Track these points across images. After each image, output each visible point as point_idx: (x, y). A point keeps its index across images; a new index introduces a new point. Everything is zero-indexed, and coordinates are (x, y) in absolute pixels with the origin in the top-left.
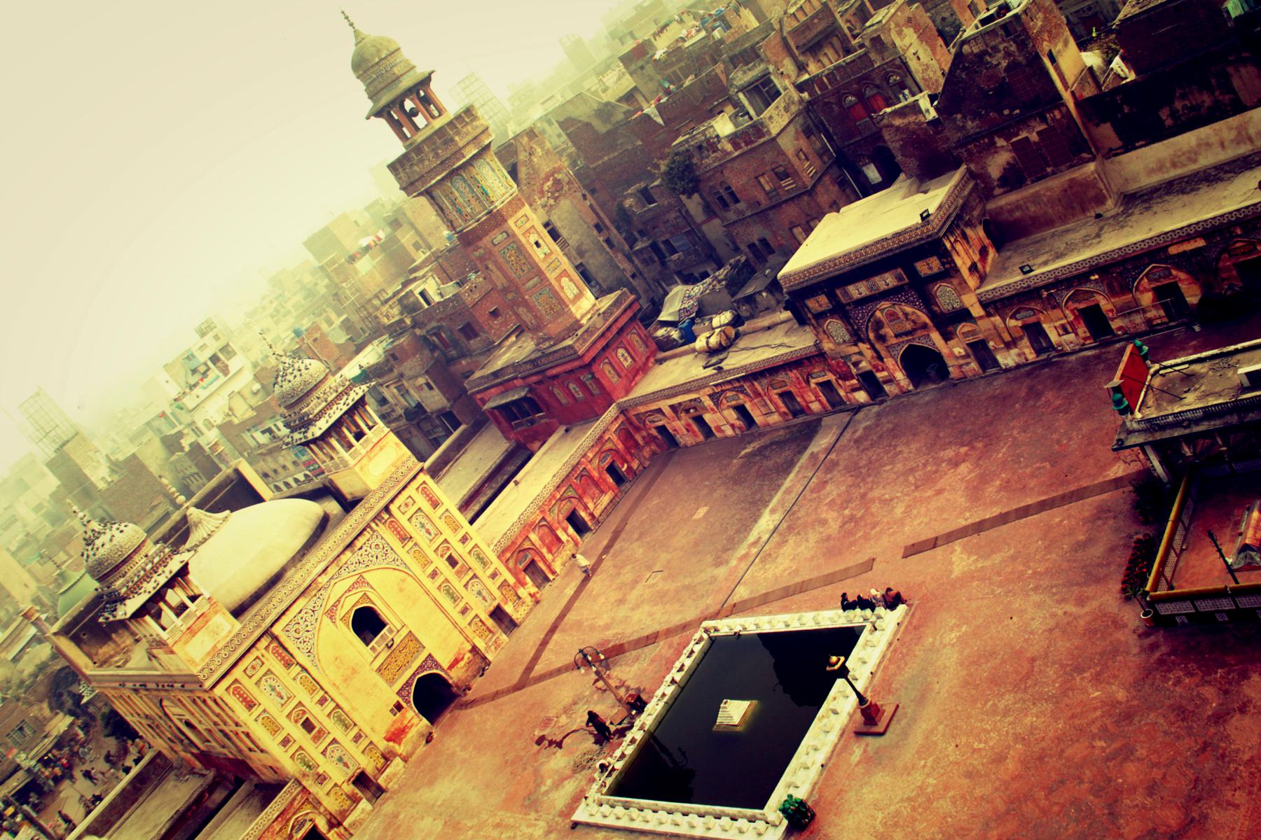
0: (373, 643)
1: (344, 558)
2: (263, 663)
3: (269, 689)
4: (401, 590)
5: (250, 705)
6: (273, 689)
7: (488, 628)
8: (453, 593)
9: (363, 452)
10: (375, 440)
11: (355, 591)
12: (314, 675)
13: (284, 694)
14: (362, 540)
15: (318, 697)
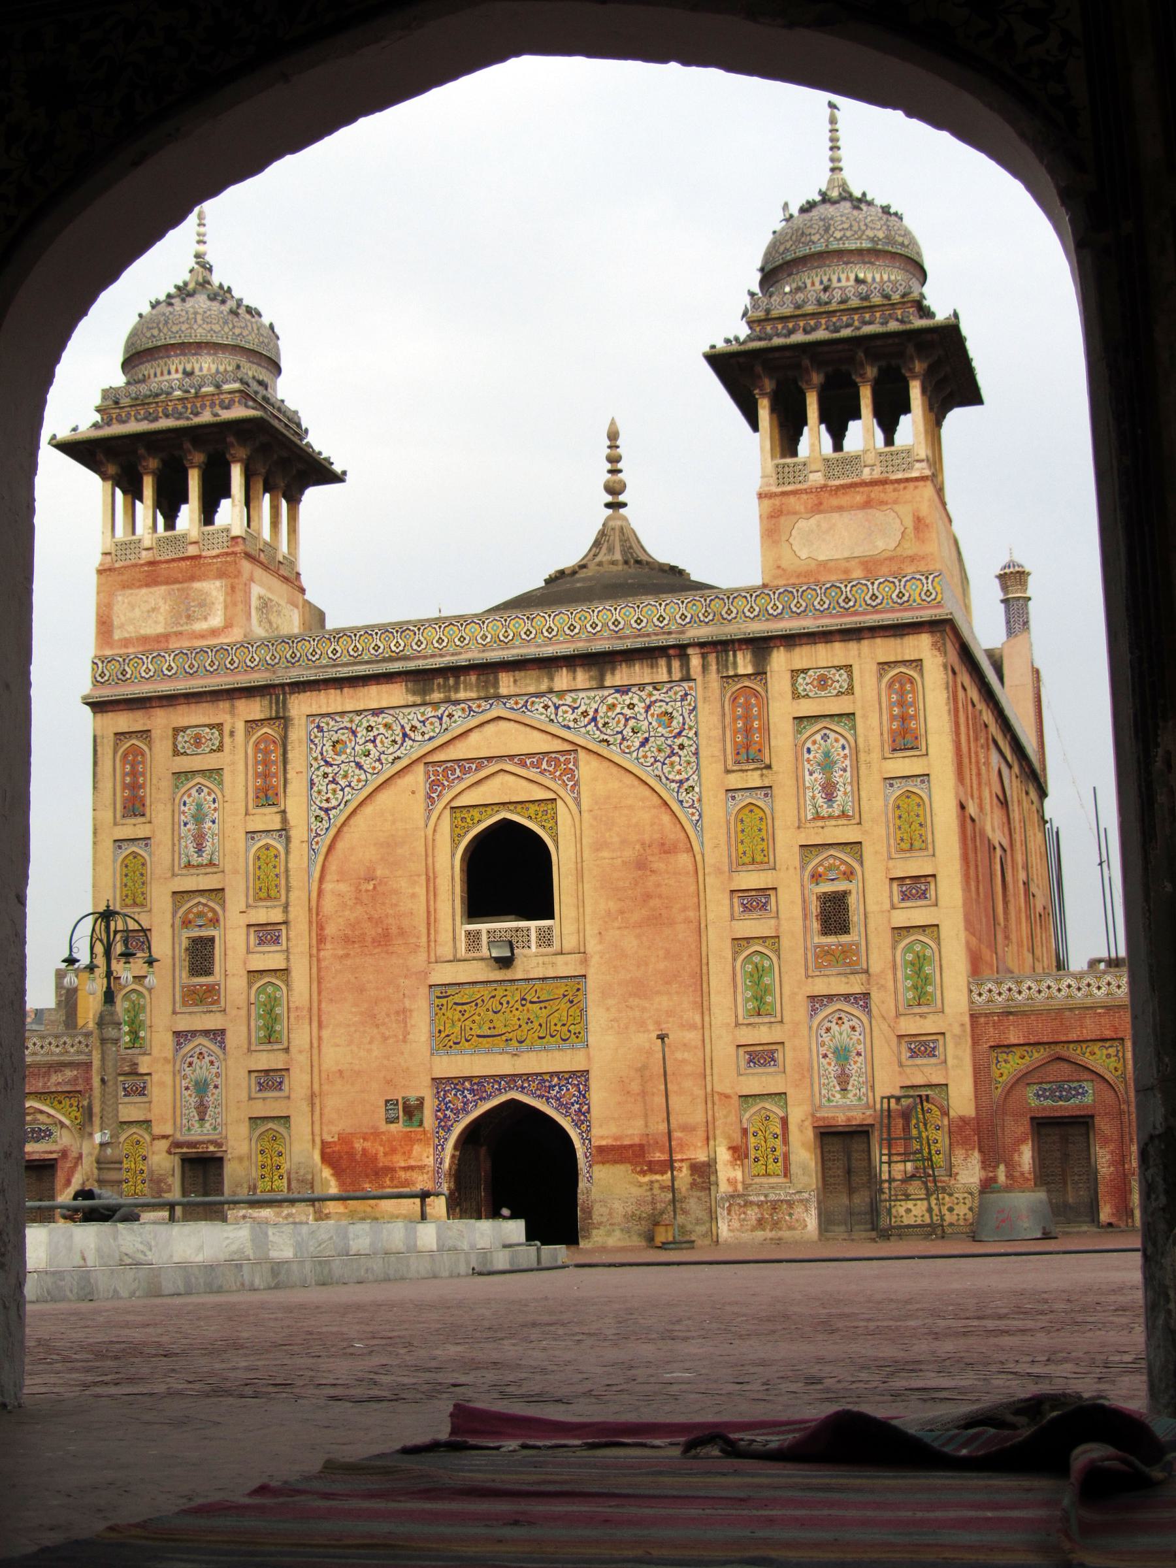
0: (483, 927)
1: (562, 679)
2: (220, 749)
3: (190, 809)
4: (641, 865)
5: (134, 806)
6: (199, 818)
7: (786, 1157)
8: (767, 990)
9: (816, 479)
10: (866, 474)
11: (532, 773)
12: (290, 865)
13: (208, 849)
14: (638, 673)
15: (262, 915)
